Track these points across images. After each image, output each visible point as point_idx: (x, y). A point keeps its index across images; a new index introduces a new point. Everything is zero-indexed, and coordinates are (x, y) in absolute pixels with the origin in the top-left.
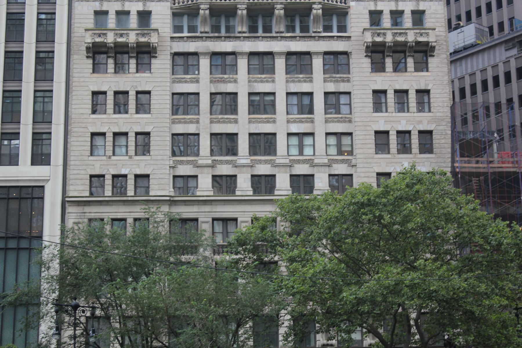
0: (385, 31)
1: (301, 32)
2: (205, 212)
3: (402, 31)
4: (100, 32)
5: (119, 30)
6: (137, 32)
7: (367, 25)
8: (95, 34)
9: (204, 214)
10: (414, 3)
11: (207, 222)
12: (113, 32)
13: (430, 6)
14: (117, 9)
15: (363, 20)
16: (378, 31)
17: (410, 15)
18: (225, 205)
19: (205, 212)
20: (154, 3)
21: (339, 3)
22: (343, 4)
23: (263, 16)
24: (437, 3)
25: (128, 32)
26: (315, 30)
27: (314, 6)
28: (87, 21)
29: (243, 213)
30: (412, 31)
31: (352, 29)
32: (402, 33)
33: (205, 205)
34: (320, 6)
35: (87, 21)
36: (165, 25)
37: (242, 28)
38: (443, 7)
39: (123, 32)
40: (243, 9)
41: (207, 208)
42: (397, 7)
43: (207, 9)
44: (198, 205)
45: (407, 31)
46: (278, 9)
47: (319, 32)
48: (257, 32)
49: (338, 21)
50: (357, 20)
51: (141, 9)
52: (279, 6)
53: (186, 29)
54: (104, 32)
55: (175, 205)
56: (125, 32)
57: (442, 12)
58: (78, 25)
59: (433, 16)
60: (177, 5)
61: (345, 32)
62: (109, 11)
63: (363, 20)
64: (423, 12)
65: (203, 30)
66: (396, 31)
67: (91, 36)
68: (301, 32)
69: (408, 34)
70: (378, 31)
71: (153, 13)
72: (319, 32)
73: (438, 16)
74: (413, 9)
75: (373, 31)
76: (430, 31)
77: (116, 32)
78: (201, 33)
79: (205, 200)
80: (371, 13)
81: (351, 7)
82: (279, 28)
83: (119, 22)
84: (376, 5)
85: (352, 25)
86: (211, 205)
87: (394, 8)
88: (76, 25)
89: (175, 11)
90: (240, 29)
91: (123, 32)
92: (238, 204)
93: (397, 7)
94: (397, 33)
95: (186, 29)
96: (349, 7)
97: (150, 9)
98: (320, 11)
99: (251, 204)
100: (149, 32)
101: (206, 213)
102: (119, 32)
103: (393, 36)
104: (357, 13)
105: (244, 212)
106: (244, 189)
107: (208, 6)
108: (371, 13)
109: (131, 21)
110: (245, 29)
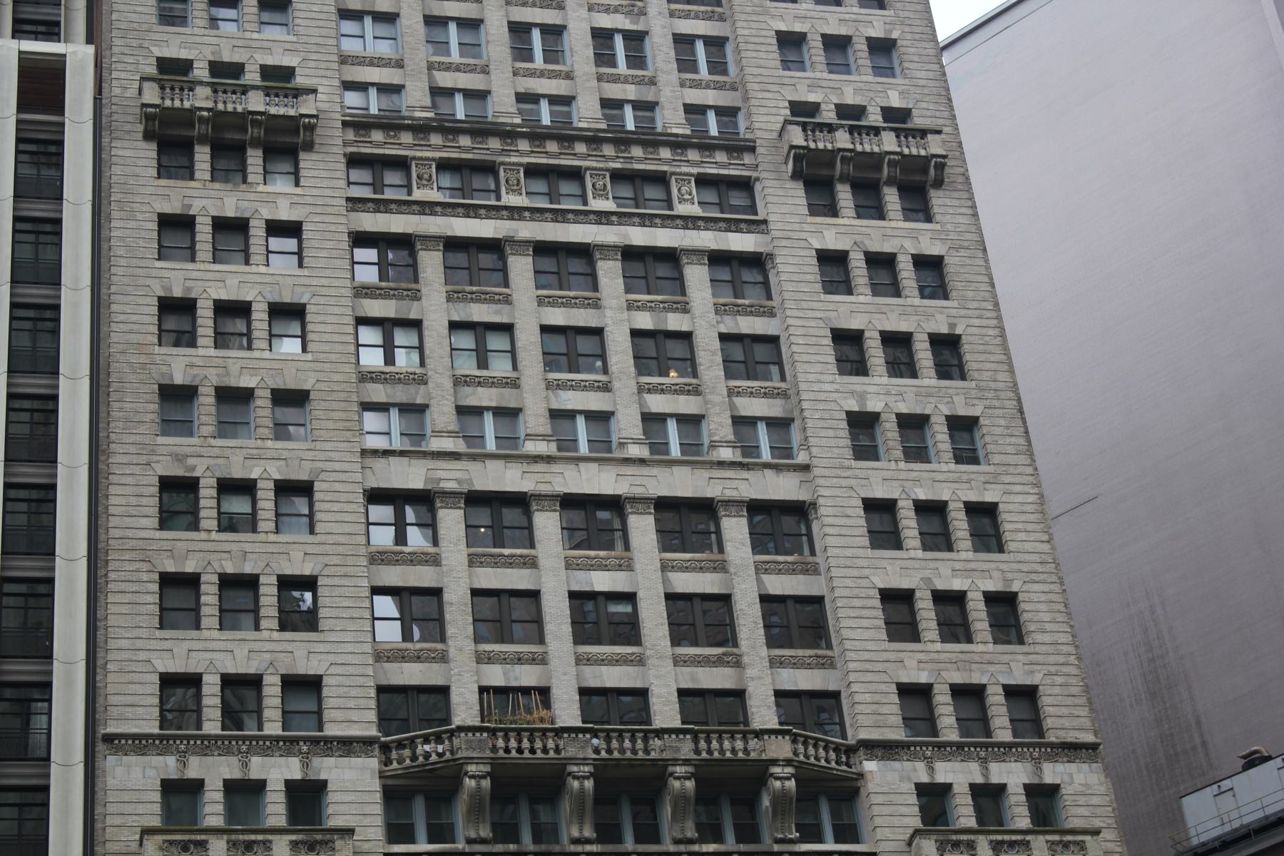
0: (972, 837)
1: (738, 841)
3: (1014, 838)
4: (186, 837)
5: (243, 832)
6: (294, 837)
7: (917, 822)
8: (171, 843)
10: (1029, 766)
12: (225, 837)
13: (1071, 775)
14: (228, 777)
15: (904, 810)
16: (954, 837)
17: (1024, 798)
20: (333, 759)
21: (833, 764)
22: (844, 768)
23: (634, 802)
24: (1085, 766)
25: (270, 837)
26: (780, 836)
27: (776, 770)
28: (141, 809)
30: (1041, 838)
31: (880, 834)
32: (1015, 842)
34: (789, 770)
35: (141, 809)
36: (367, 821)
37: (581, 830)
38: (1103, 778)
39: (253, 837)
40: (584, 778)
42: (986, 776)
43: (484, 777)
45: (1028, 838)
46: (678, 778)
47: (792, 841)
48: (620, 840)
49: (835, 815)
50: (887, 810)
51: (297, 775)
52: (680, 770)
53: (421, 831)
54: (199, 837)
56: (260, 837)
57: (1103, 789)
58: (118, 821)
59: (1082, 800)
60: (395, 765)
61: (856, 840)
62: (206, 782)
63: (904, 810)
64: (1054, 790)
65: (473, 835)
66: (999, 838)
67: (161, 849)
68: (738, 841)
69: (1033, 845)
70: (954, 837)
71: (330, 787)
72: (792, 841)
73: (1095, 800)
74: (1027, 781)
75: (941, 838)
76: (1087, 838)
77: (233, 837)
78: (470, 841)
80: (921, 789)
81: (869, 777)
82: (683, 830)
83: (231, 812)
84: (931, 770)
85: (878, 821)
87: (979, 779)
88: (109, 820)
89: (390, 782)
90: (575, 833)
91: (253, 837)
93: (986, 776)
94: (1002, 842)
95: (421, 831)
96: (861, 775)
97: (323, 777)
98: (792, 784)
100: (328, 837)
102: (241, 837)
103: (993, 849)
104: (885, 789)
107: (488, 768)
108: (921, 789)
109: (270, 809)
110: (588, 832)
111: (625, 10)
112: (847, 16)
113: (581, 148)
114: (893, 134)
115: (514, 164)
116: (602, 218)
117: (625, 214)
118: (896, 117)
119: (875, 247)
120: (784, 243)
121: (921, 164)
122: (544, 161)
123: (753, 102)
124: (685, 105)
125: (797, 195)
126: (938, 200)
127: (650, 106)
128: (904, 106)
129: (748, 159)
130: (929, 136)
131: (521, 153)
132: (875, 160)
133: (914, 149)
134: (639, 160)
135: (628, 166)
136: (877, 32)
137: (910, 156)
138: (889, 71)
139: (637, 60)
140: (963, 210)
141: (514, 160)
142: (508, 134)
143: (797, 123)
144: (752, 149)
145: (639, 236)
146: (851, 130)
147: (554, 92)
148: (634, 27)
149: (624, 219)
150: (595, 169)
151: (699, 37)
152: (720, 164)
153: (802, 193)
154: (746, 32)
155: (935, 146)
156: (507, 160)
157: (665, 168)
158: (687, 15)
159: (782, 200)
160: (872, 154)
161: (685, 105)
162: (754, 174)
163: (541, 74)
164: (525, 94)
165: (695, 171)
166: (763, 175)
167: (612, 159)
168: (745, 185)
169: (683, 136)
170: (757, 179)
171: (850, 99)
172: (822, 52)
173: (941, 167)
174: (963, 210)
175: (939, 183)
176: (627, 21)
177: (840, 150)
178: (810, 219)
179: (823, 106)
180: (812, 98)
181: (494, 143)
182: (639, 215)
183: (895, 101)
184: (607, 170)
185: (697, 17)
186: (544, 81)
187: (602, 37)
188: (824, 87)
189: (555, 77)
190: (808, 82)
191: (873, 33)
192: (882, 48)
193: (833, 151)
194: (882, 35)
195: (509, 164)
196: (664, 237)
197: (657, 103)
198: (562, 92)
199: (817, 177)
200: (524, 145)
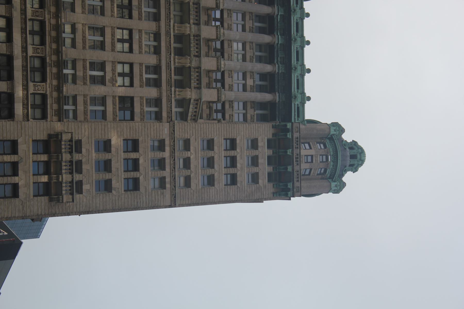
111: (114, 78)
112: (120, 172)
113: (54, 46)
114: (70, 180)
115: (45, 16)
116: (25, 49)
117: (27, 59)
118: (78, 187)
119: (20, 166)
120: (19, 126)
121: (59, 193)
122: (47, 29)
123: (80, 124)
124: (76, 95)
125: (43, 136)
126: (44, 199)
127: (74, 81)
128: (83, 190)
129: (55, 118)
130: (71, 196)
131: (49, 20)
132: (59, 172)
133: (65, 188)
134: (51, 70)
135: (48, 65)
136: (114, 184)
137: (62, 187)
138: (98, 189)
139: (94, 80)
140: (40, 211)
141: (47, 16)
142: (57, 16)
143: (72, 138)
144: (59, 120)
145: (18, 63)
146: (71, 162)
147: (77, 40)
148: (107, 81)
149: (25, 58)
150: (45, 50)
151: (106, 108)
152: (51, 106)
153: (42, 138)
154: (109, 126)
155: (66, 197)
156: (46, 12)
157: (48, 81)
158: (114, 104)
159: (39, 130)
160: (61, 169)
161: (76, 95)
162: (49, 119)
163: (84, 37)
164: (75, 28)
165: (48, 93)
166: (49, 123)
167: (51, 59)
168: (44, 117)
169: (63, 90)
170: (47, 121)
171: (84, 167)
172: (103, 158)
173: (58, 201)
174: (40, 211)
175: (51, 200)
176: (109, 78)
177: (62, 154)
178: (31, 140)
179: (80, 155)
180: (84, 150)
181: (53, 9)
182: (27, 73)
183: (86, 187)
184: (46, 55)
185: (114, 108)
186: (81, 37)
187: (102, 66)
188: (90, 156)
189: (83, 42)
190: (90, 149)
191: (114, 182)
192: (107, 186)
193: (61, 152)
194: (113, 186)
195: (45, 13)
196: (18, 74)
197: (76, 84)
198: (77, 44)
199: (50, 145)
200: (53, 21)
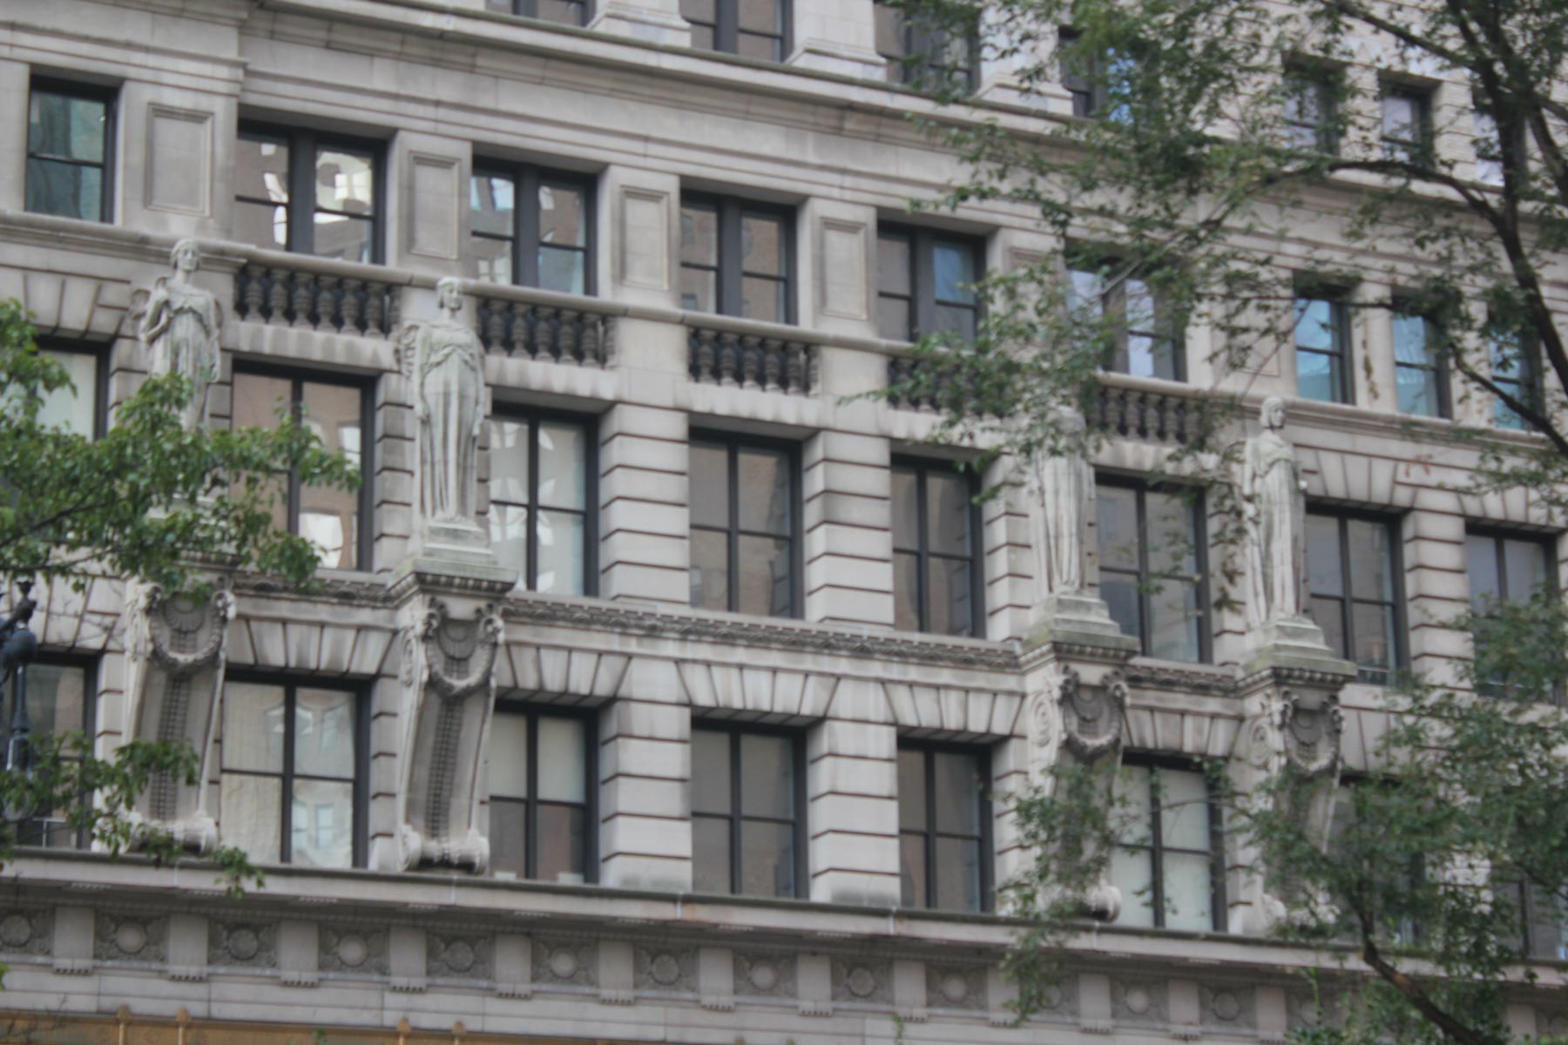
2: (438, 104)
9: (430, 112)
11: (444, 163)
18: (541, 81)
19: (438, 104)
29: (638, 146)
33: (436, 63)
41: (448, 86)
44: (399, 57)
55: (272, 35)
79: (441, 36)
86: (472, 69)
92: (611, 93)
99: (680, 105)
101: (442, 113)
105: (646, 139)
106: (644, 17)
